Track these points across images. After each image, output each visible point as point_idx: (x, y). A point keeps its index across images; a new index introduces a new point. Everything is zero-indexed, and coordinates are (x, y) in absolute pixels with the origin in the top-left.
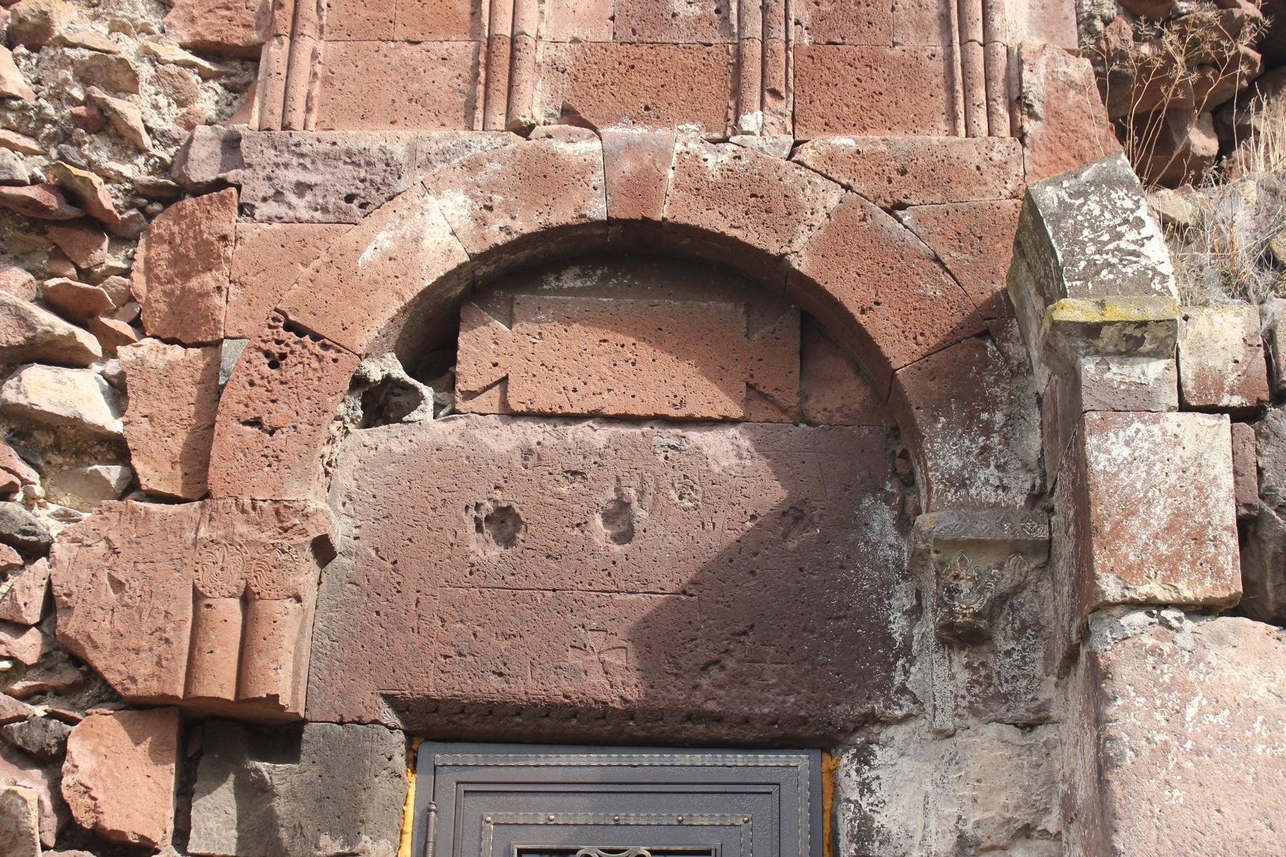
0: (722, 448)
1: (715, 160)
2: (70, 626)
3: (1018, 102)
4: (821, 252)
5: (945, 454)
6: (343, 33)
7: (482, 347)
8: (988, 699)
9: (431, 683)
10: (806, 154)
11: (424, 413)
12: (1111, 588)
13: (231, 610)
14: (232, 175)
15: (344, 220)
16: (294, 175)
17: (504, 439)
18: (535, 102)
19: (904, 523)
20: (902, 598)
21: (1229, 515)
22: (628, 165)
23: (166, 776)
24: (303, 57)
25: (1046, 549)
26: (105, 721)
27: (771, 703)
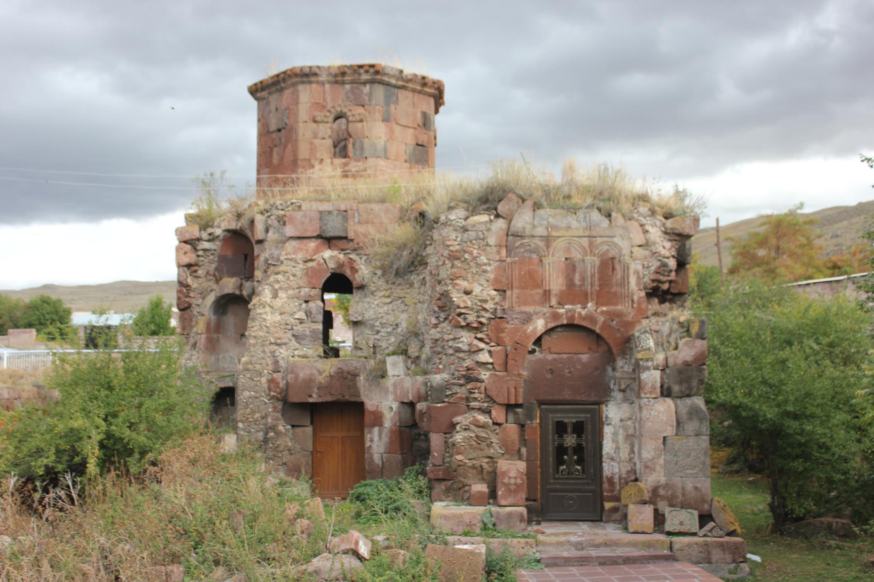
0: (585, 358)
1: (583, 312)
2: (489, 393)
3: (633, 301)
4: (601, 328)
5: (620, 363)
6: (520, 288)
7: (545, 341)
8: (625, 400)
9: (541, 397)
10: (599, 310)
11: (537, 353)
12: (643, 395)
13: (513, 390)
14: (505, 316)
15: (524, 324)
16: (514, 316)
17: (550, 357)
18: (554, 302)
19: (614, 369)
20: (612, 382)
21: (659, 385)
22: (569, 314)
23: (504, 412)
24: (514, 295)
25: (634, 379)
26: (496, 406)
27: (593, 399)
